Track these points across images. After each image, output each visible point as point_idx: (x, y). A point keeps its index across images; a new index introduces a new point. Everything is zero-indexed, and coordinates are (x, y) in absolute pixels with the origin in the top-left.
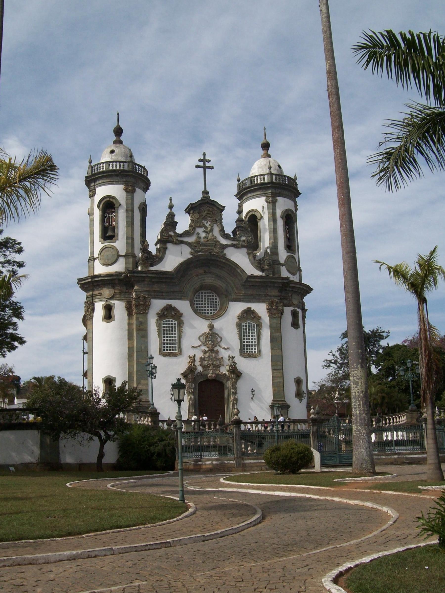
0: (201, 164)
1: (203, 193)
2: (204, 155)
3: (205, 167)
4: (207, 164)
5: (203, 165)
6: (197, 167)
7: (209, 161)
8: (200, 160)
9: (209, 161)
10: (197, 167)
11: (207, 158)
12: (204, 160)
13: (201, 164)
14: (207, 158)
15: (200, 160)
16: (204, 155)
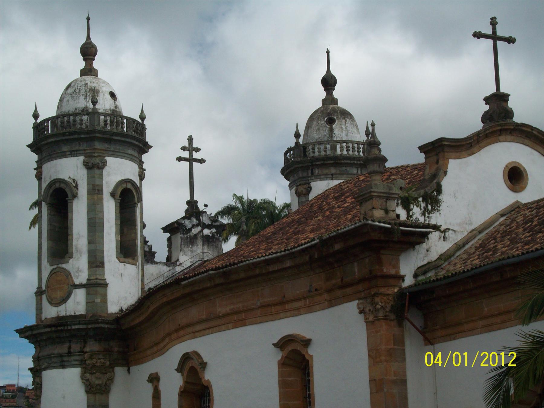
0: (186, 154)
1: (188, 203)
2: (190, 139)
3: (191, 160)
4: (196, 155)
5: (188, 157)
6: (180, 159)
7: (197, 150)
8: (184, 149)
9: (197, 150)
10: (180, 159)
11: (194, 146)
12: (191, 148)
13: (186, 154)
14: (194, 146)
15: (184, 149)
16: (190, 139)
